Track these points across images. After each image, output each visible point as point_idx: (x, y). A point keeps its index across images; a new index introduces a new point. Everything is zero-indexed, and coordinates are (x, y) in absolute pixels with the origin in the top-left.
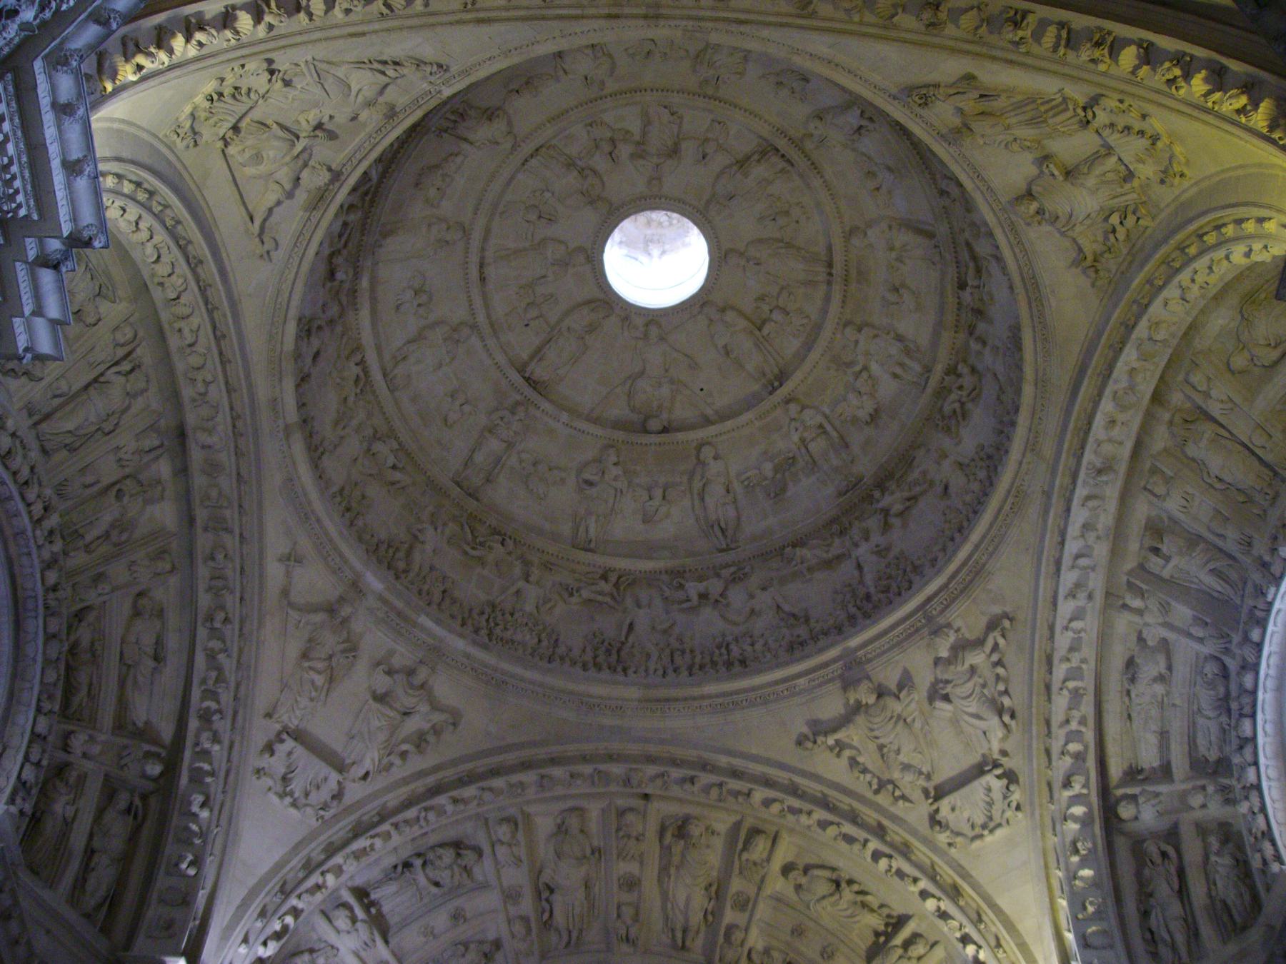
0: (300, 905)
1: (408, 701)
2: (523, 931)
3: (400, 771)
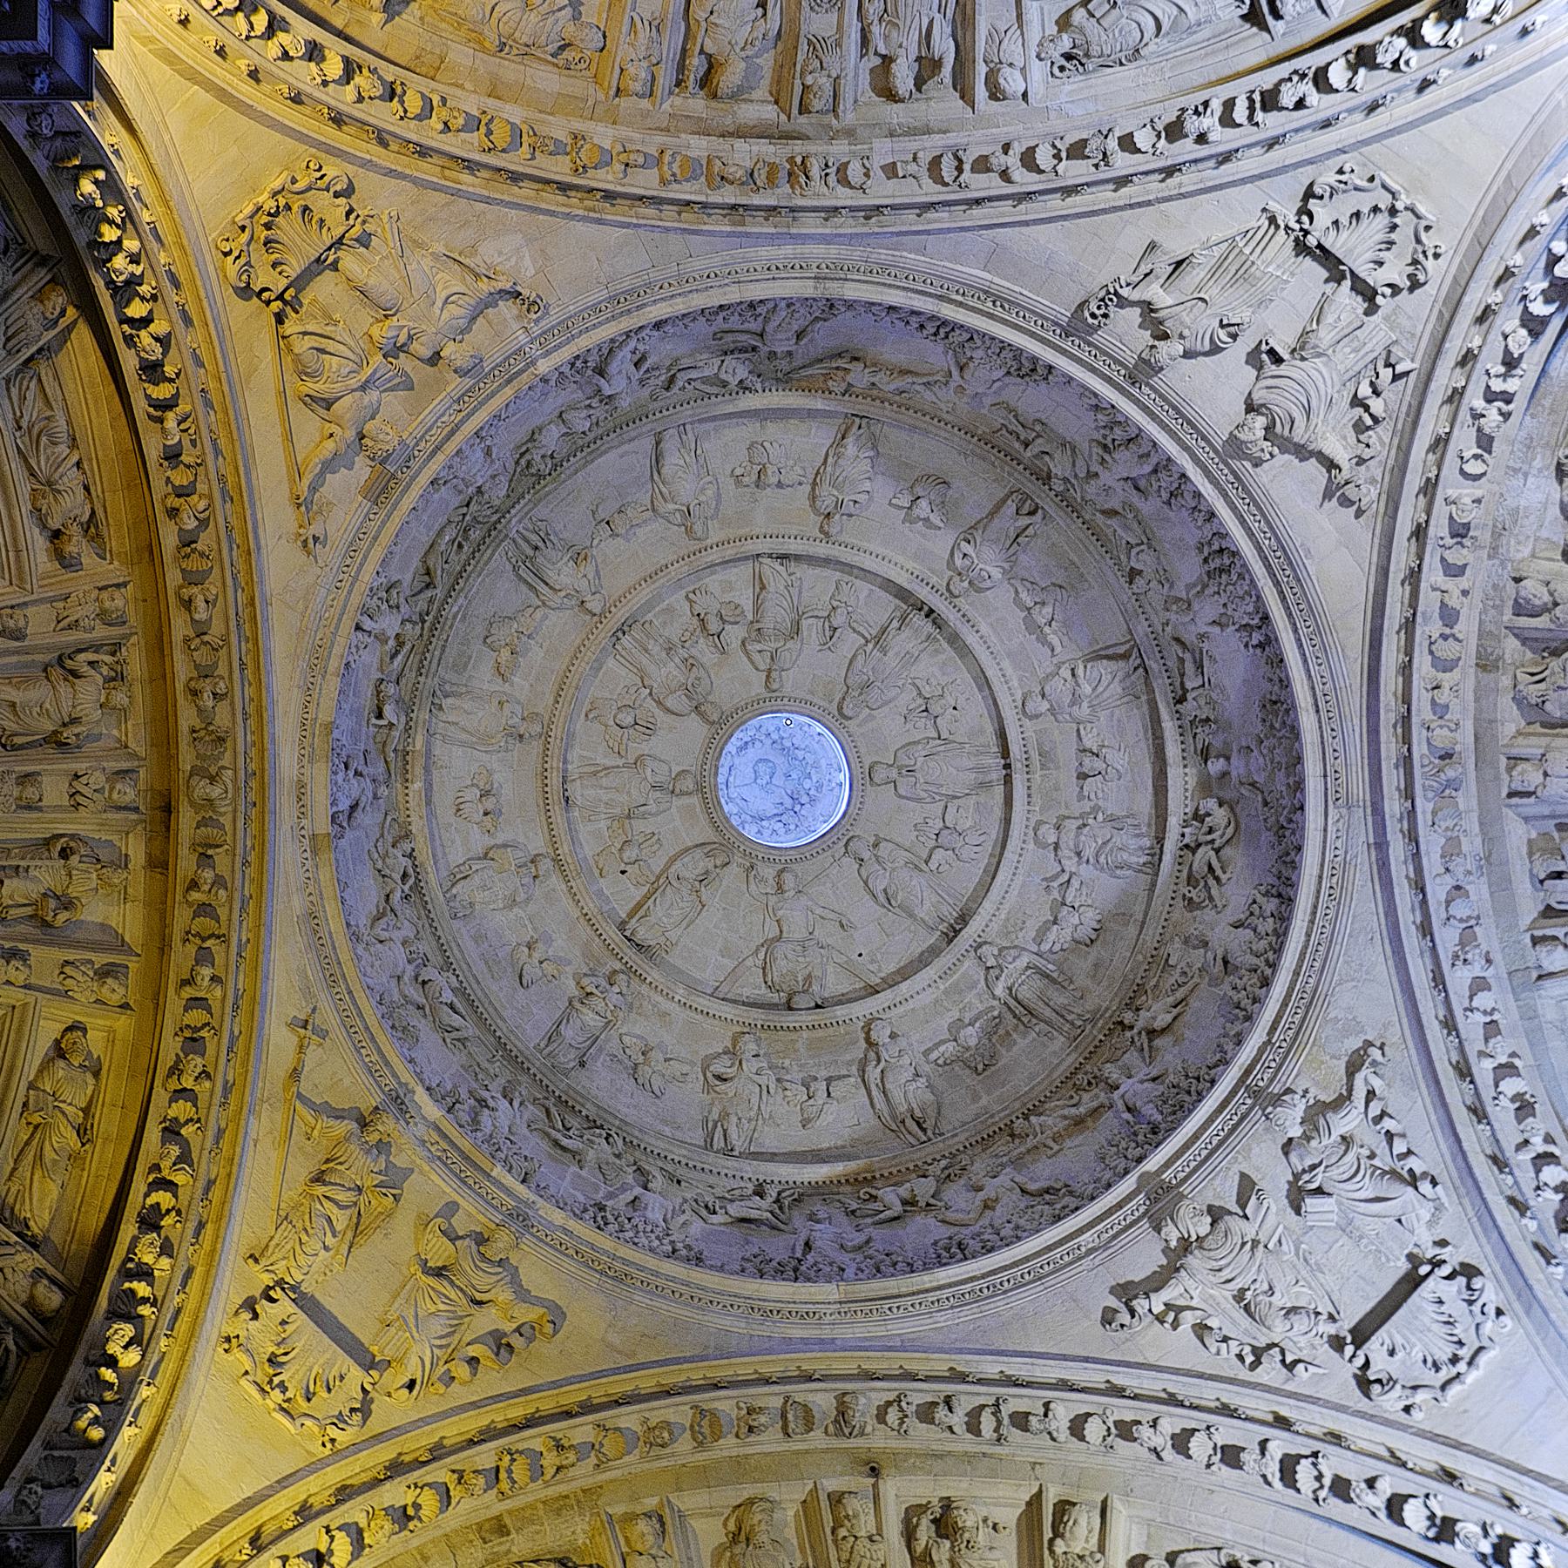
1: (482, 1280)
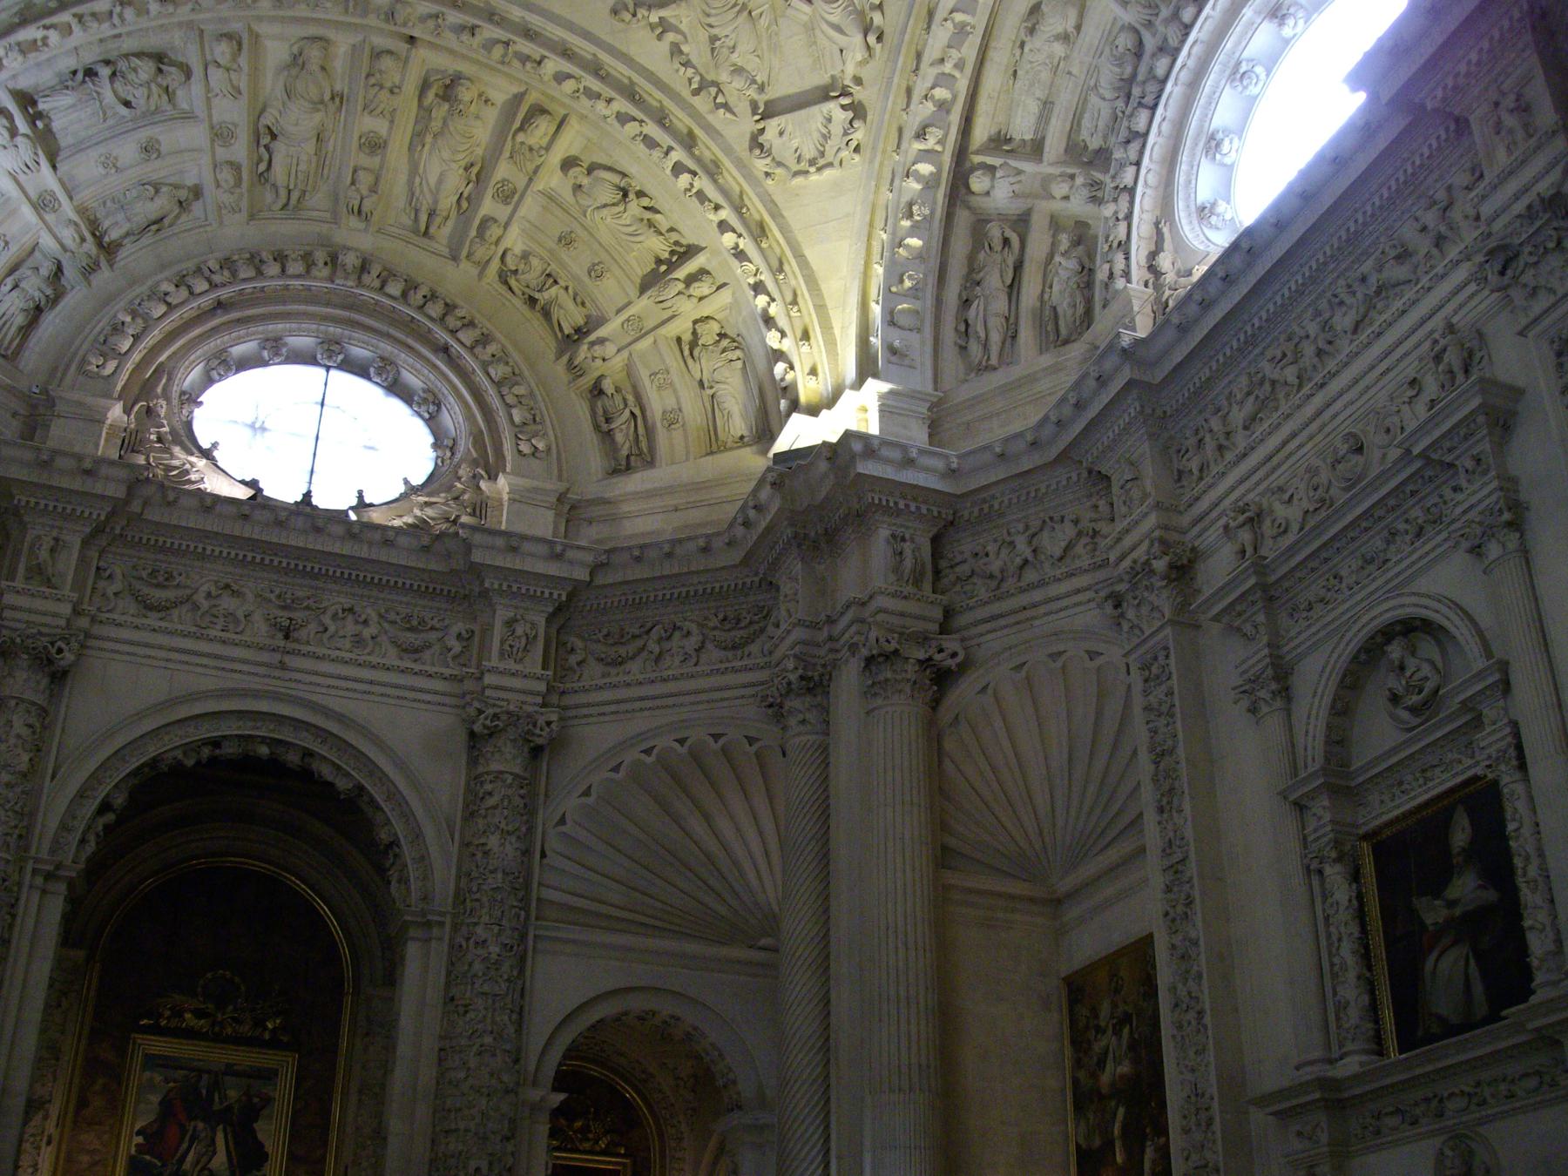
2: (232, 183)
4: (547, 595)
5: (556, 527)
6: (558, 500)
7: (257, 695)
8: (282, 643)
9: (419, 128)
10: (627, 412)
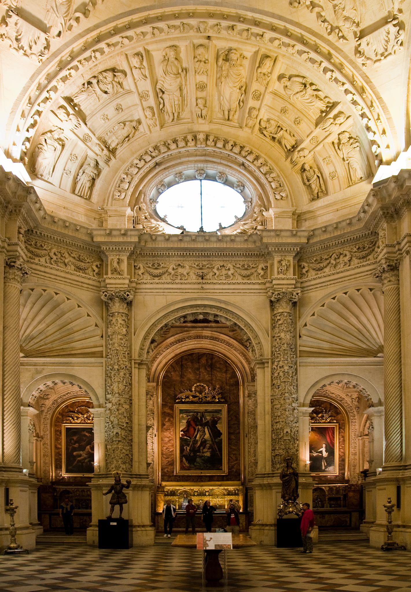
0: (40, 109)
2: (151, 115)
3: (77, 29)
4: (292, 250)
5: (293, 224)
6: (293, 214)
7: (195, 299)
8: (201, 281)
9: (218, 76)
10: (315, 176)
